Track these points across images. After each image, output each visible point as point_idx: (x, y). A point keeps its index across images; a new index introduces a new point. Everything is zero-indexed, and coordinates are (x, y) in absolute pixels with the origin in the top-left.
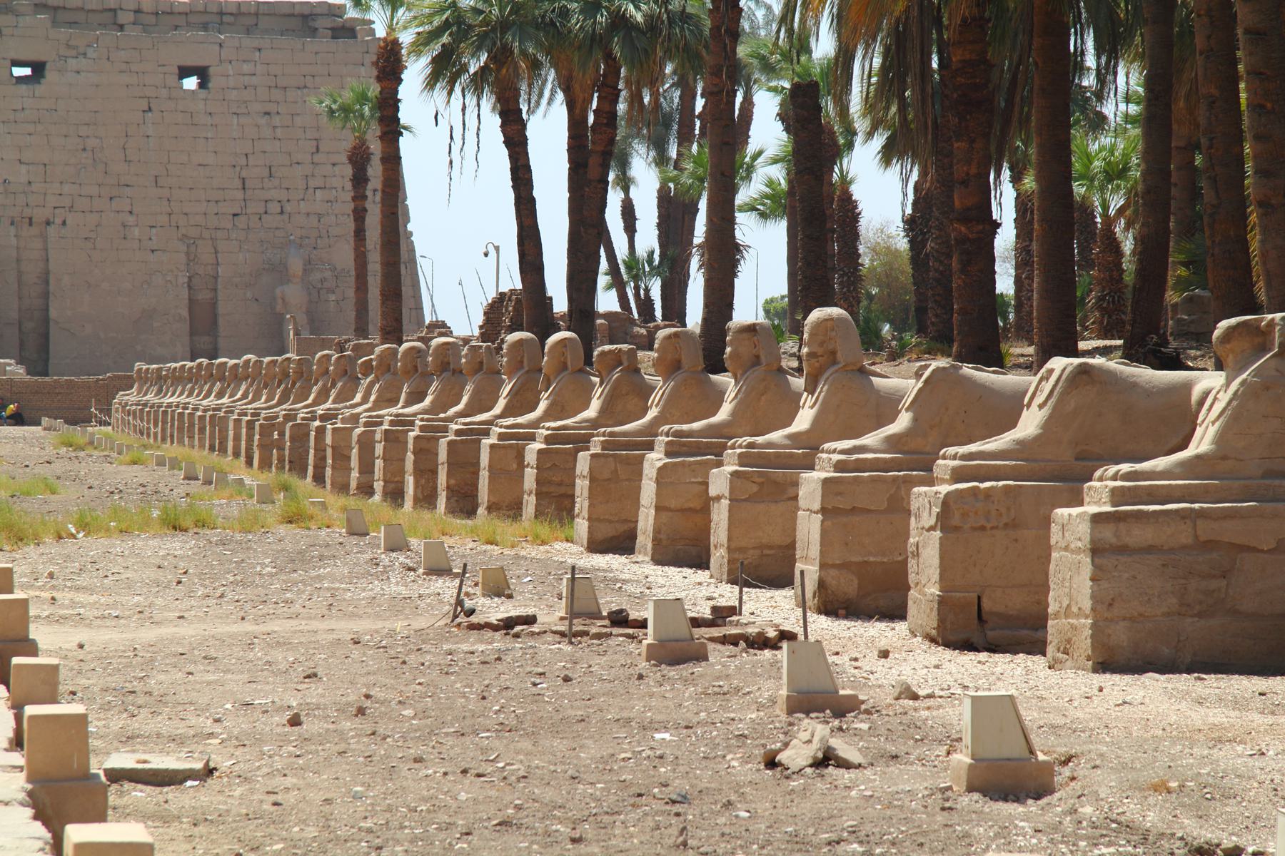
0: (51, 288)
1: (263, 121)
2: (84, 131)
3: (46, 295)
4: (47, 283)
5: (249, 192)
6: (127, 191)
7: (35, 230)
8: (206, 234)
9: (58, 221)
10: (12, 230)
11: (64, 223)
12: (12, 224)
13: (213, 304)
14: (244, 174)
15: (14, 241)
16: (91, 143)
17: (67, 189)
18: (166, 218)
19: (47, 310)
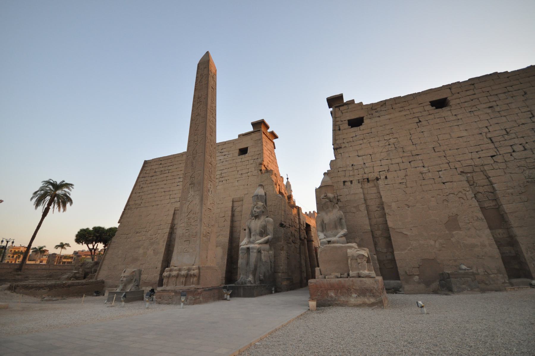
0: (387, 211)
1: (489, 111)
2: (387, 138)
3: (384, 215)
4: (383, 209)
5: (497, 144)
6: (420, 157)
7: (371, 184)
8: (477, 169)
9: (383, 177)
10: (360, 185)
11: (386, 178)
12: (359, 182)
13: (498, 208)
14: (489, 135)
15: (361, 190)
16: (392, 141)
17: (384, 162)
18: (447, 165)
19: (387, 223)
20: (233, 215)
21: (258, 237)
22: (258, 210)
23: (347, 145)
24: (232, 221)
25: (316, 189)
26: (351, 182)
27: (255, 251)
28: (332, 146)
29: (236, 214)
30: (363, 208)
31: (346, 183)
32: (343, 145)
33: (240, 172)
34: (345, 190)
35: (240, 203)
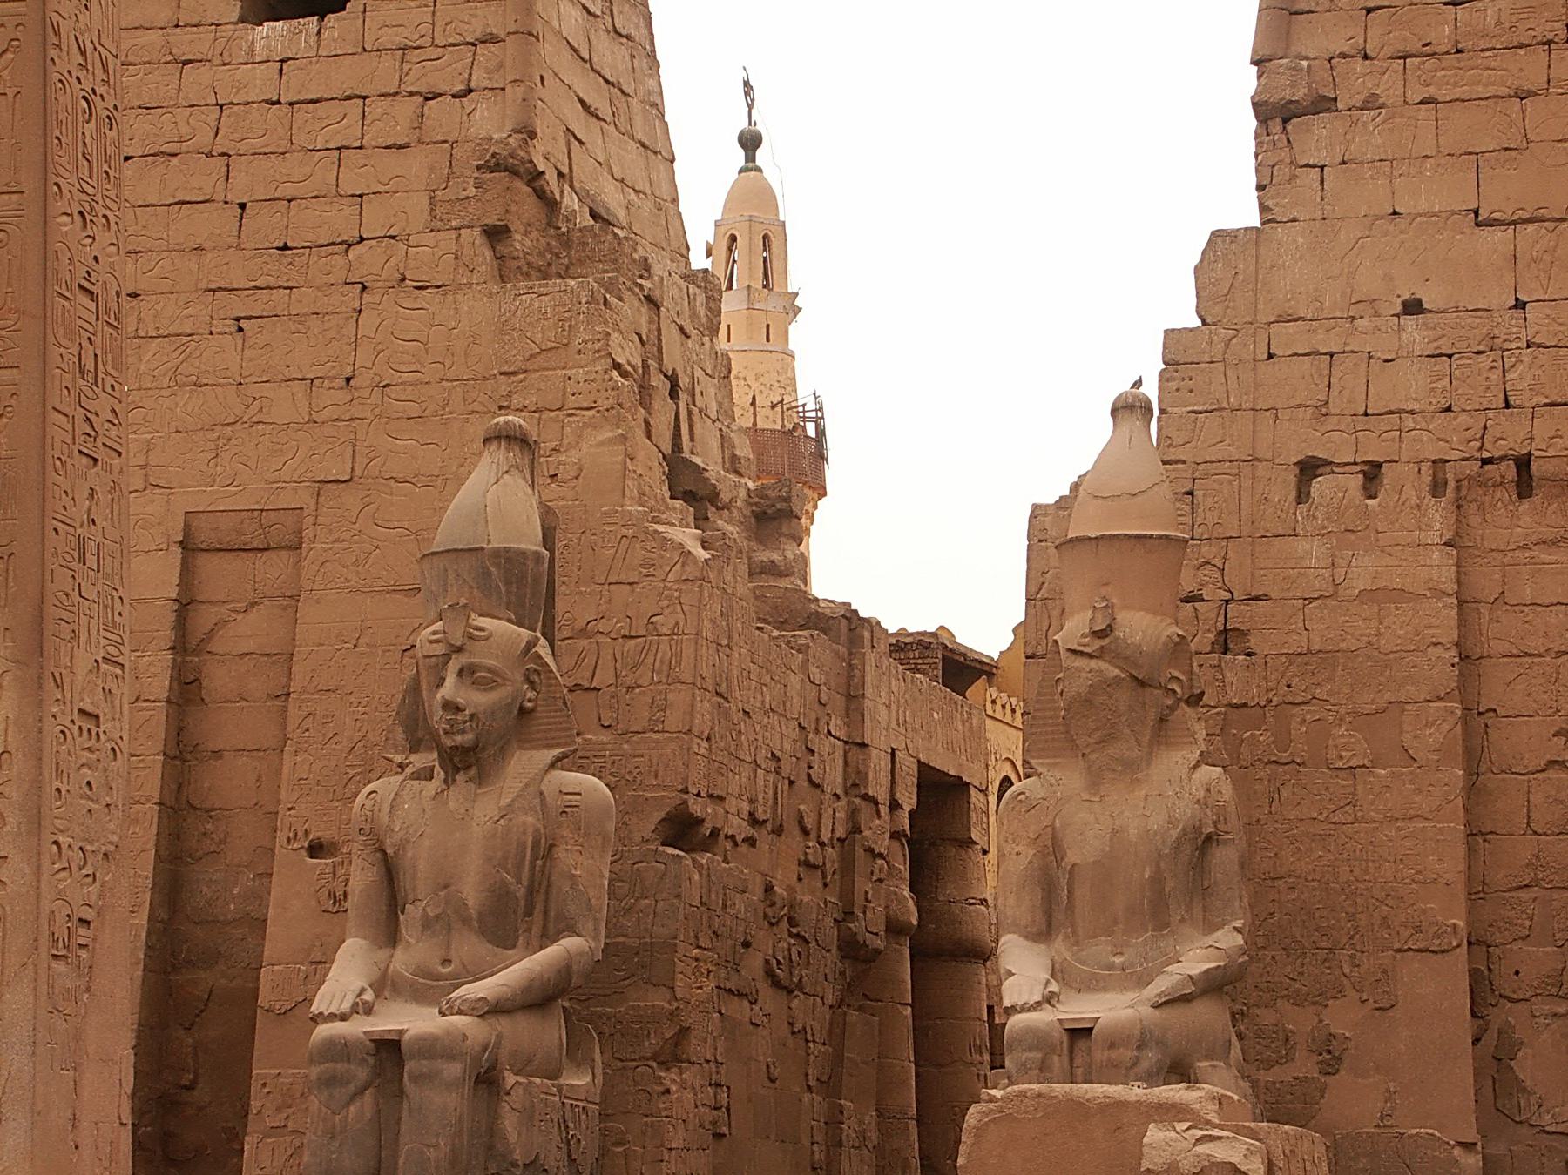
12: (1437, 488)
20: (187, 691)
21: (469, 946)
22: (477, 700)
23: (1389, 86)
24: (182, 752)
25: (1037, 512)
26: (1372, 474)
27: (453, 1070)
28: (1248, 80)
29: (219, 678)
30: (1435, 729)
31: (1321, 485)
32: (1356, 82)
33: (266, 225)
34: (1301, 546)
35: (273, 569)
